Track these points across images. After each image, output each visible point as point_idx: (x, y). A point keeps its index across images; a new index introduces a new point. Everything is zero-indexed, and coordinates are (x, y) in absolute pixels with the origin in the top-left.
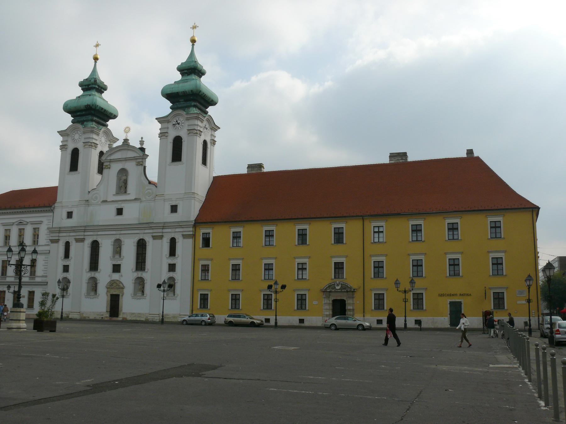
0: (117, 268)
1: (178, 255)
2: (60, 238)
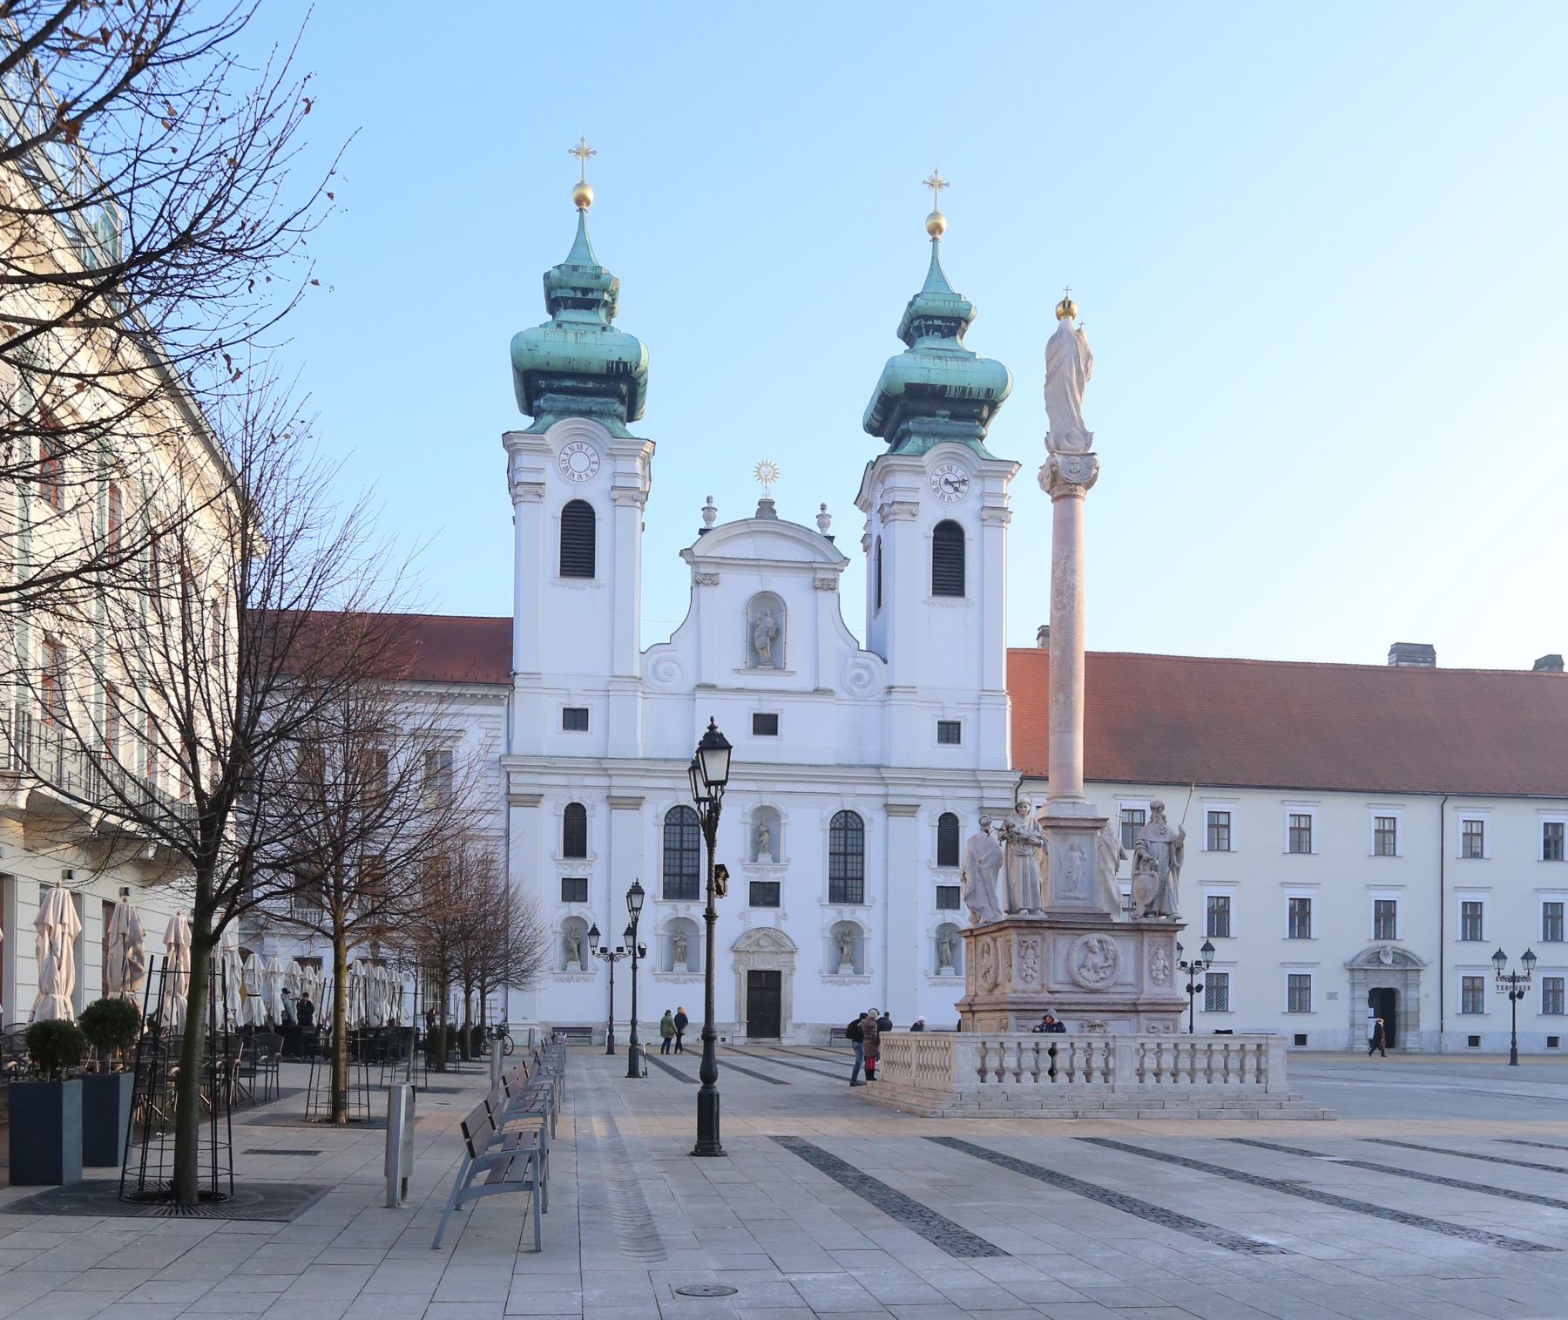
0: (765, 894)
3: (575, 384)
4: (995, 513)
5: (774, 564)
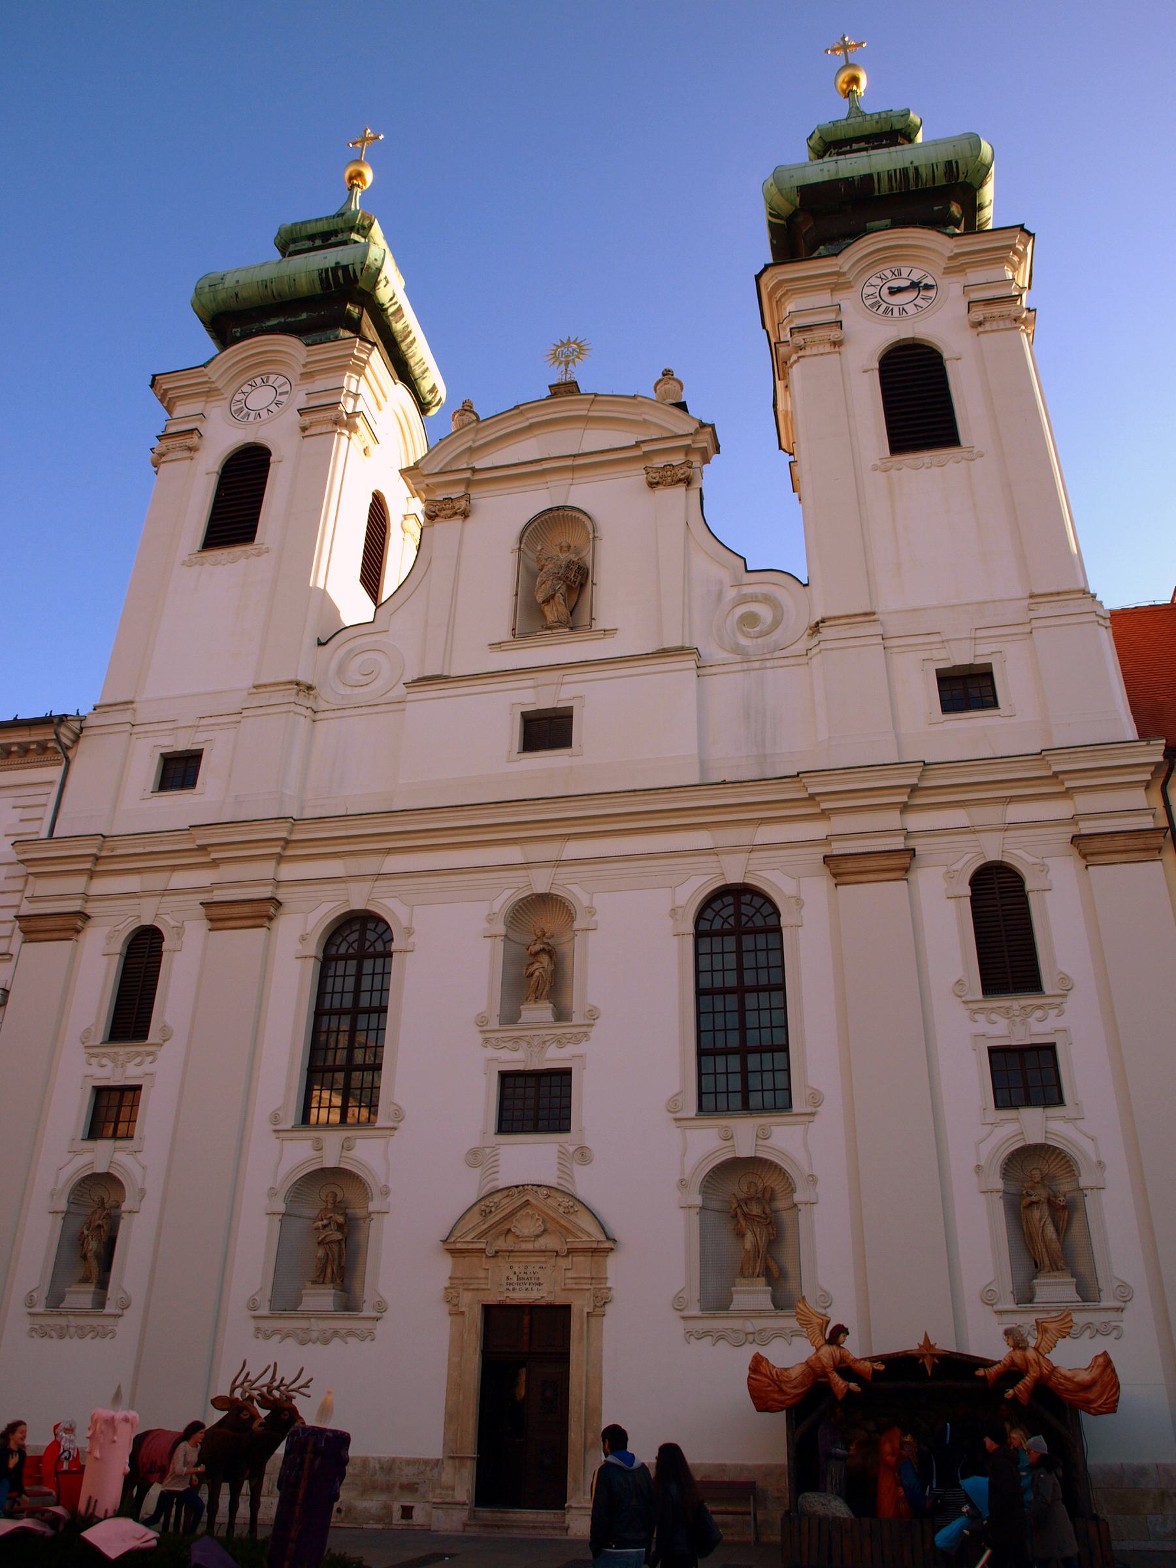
1: (1065, 978)
2: (90, 909)
3: (282, 320)
4: (996, 310)
5: (569, 462)
